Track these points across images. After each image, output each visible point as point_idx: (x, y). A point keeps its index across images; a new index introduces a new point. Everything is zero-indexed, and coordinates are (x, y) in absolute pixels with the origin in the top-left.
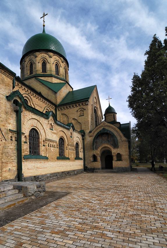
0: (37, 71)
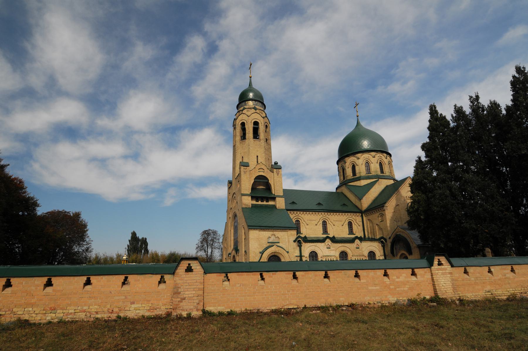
0: (347, 176)
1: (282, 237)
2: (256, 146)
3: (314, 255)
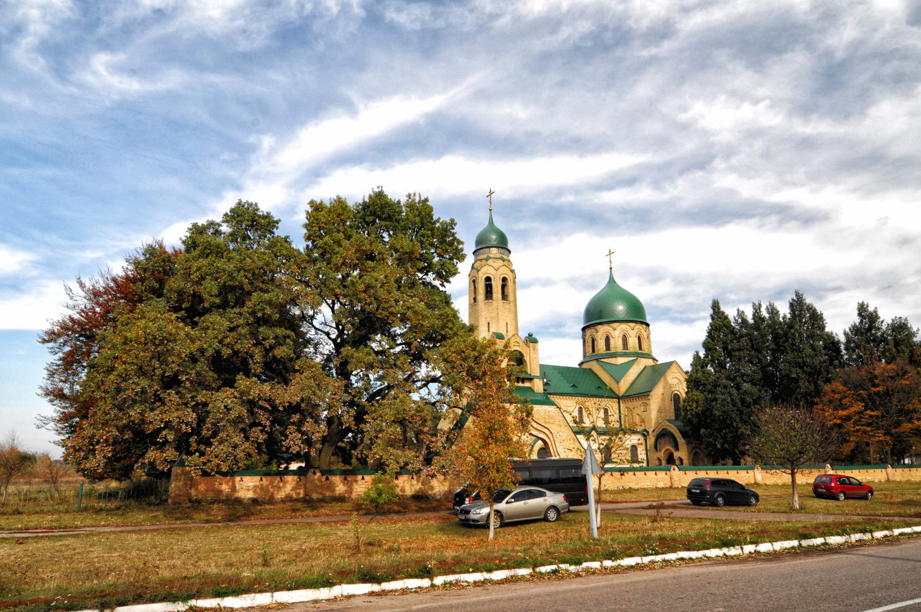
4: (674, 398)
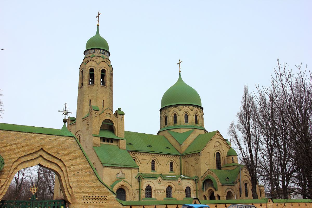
0: (169, 123)
1: (128, 174)
2: (103, 92)
3: (149, 189)
4: (216, 155)
